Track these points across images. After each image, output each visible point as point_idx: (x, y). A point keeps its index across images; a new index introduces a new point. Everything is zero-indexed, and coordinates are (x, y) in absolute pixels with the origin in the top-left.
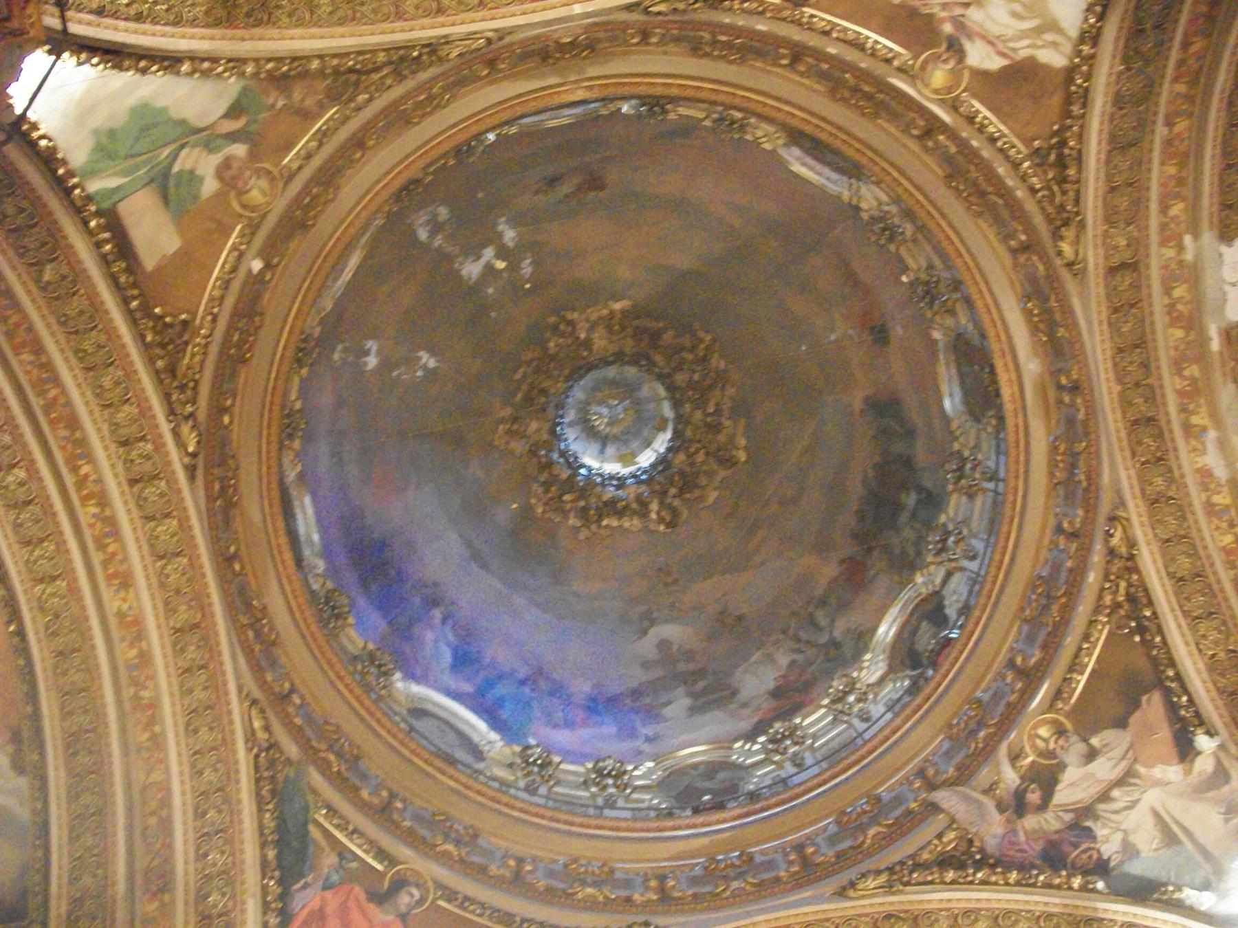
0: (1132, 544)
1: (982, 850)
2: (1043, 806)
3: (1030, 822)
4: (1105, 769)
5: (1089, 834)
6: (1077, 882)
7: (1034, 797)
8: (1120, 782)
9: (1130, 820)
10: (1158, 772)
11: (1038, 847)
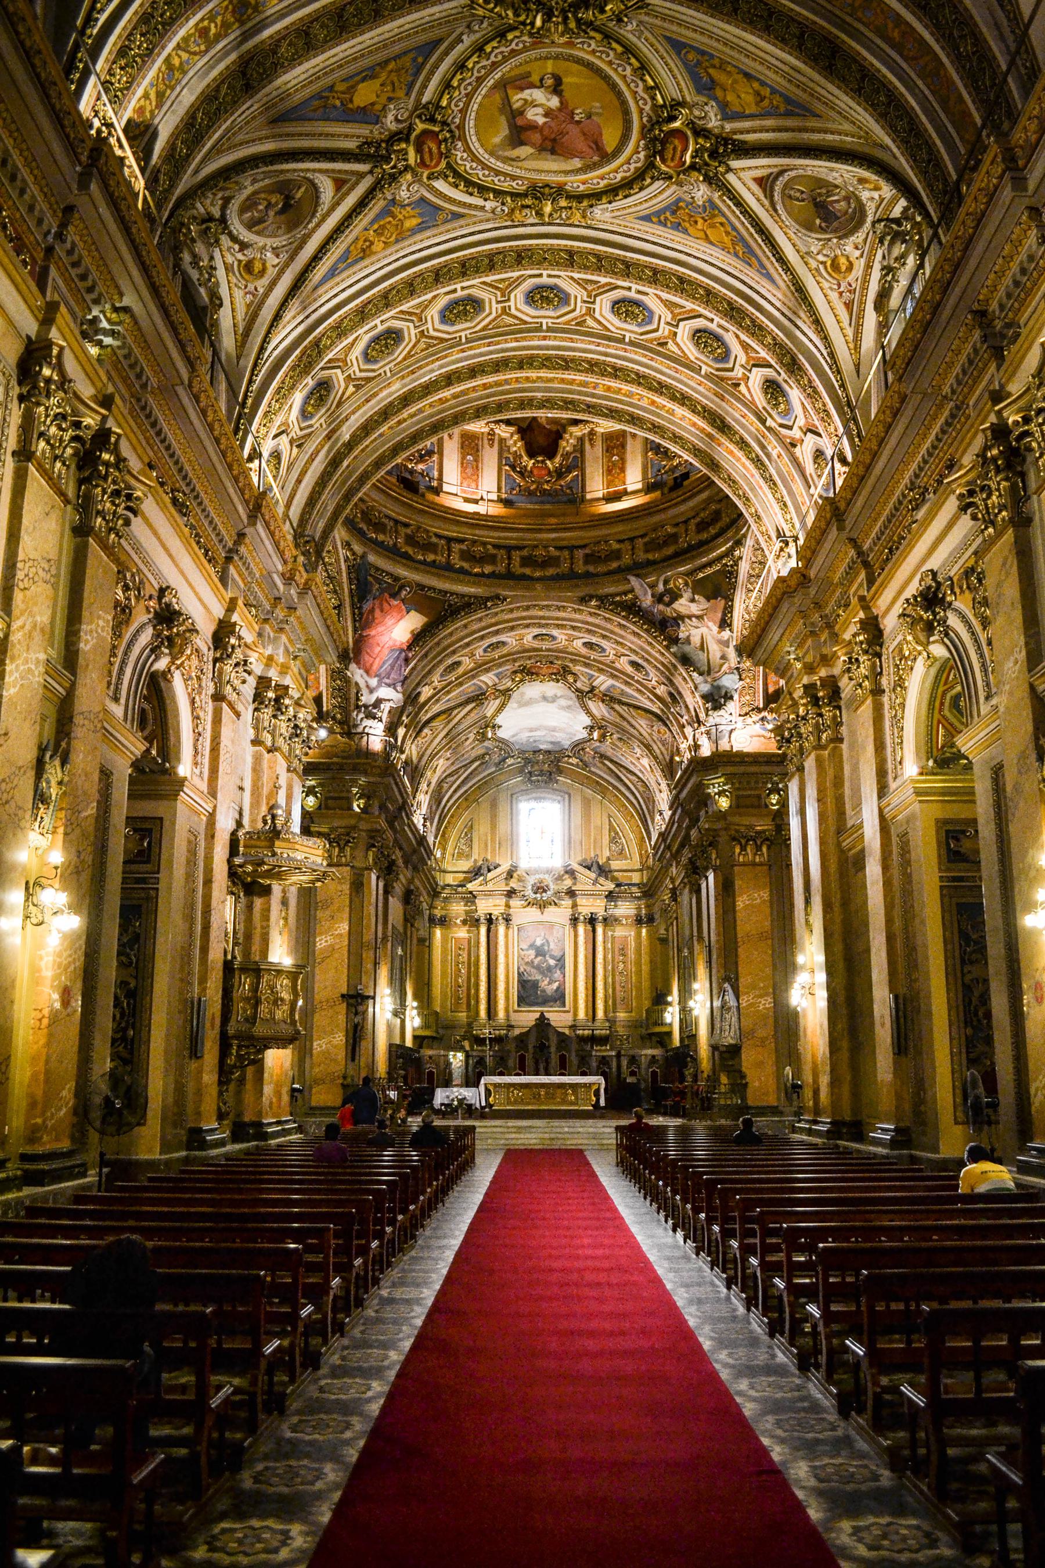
0: (741, 558)
2: (668, 605)
3: (661, 607)
4: (694, 609)
5: (678, 625)
7: (666, 599)
8: (698, 617)
9: (693, 632)
10: (710, 624)
11: (660, 617)
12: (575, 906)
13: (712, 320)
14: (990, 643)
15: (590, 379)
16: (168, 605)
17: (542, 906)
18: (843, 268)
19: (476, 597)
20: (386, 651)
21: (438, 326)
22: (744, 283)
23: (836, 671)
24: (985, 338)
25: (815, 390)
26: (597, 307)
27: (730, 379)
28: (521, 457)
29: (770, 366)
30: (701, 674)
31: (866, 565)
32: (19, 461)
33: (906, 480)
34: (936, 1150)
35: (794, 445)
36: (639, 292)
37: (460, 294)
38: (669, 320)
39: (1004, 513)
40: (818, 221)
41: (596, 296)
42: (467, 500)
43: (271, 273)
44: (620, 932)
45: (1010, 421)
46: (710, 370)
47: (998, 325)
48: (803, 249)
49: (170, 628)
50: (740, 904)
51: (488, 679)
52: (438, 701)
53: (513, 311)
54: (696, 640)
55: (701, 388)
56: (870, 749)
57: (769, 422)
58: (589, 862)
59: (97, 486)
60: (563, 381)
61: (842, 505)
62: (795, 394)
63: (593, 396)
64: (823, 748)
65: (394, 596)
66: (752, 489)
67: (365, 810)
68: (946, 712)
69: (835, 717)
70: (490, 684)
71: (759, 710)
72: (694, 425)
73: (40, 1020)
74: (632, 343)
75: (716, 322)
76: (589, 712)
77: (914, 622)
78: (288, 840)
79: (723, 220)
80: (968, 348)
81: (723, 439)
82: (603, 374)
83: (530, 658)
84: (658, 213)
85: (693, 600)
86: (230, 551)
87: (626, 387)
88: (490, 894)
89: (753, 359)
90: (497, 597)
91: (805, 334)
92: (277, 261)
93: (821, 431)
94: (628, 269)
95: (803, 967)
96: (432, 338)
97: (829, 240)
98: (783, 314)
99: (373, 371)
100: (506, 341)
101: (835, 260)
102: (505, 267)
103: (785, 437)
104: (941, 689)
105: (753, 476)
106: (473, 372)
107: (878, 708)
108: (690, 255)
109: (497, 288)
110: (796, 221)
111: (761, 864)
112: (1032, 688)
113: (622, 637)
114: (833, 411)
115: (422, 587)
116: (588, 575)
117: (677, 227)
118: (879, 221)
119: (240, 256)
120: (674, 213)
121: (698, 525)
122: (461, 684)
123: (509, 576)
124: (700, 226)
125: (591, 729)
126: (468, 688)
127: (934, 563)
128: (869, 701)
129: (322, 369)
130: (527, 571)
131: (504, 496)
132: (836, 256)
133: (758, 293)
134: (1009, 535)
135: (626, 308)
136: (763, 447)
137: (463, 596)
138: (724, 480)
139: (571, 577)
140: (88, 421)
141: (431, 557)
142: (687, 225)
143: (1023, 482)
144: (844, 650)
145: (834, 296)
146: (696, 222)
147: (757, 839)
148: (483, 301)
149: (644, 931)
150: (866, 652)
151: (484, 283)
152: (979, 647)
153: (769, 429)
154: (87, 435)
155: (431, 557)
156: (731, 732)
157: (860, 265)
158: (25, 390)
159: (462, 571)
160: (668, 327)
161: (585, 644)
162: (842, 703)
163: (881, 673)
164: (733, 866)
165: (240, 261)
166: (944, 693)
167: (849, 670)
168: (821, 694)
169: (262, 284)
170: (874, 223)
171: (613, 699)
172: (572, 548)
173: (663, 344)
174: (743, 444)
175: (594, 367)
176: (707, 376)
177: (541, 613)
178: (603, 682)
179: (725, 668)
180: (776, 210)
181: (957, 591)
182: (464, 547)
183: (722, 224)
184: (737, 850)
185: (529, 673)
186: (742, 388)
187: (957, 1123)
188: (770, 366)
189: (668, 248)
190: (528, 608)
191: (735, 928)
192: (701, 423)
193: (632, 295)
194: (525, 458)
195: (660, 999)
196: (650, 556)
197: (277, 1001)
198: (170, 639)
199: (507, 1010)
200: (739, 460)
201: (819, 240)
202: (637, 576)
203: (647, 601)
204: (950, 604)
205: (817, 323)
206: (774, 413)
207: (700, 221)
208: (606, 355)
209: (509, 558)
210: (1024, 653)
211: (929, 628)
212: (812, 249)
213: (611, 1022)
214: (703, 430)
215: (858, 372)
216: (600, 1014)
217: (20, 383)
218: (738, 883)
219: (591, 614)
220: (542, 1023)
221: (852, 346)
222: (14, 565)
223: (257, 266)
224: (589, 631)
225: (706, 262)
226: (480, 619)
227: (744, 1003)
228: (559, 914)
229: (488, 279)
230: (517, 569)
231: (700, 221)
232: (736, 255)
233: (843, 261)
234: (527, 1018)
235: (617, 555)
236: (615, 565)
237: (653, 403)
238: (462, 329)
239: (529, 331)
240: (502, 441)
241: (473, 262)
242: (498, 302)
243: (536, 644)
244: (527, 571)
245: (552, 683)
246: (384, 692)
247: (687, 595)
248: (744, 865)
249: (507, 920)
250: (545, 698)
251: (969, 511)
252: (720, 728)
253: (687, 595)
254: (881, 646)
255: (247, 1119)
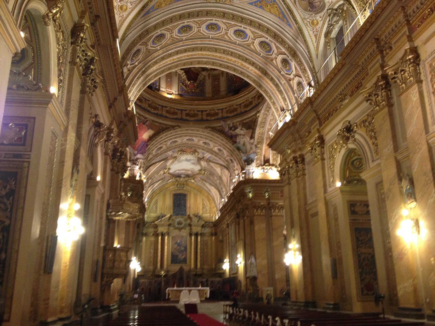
0: (259, 117)
1: (224, 131)
3: (231, 131)
4: (242, 132)
5: (236, 138)
6: (232, 143)
7: (233, 129)
8: (244, 135)
9: (241, 140)
10: (247, 137)
12: (191, 229)
13: (267, 39)
14: (373, 144)
15: (223, 56)
16: (98, 121)
17: (180, 229)
18: (315, 24)
19: (171, 126)
20: (140, 143)
21: (177, 34)
22: (280, 27)
23: (304, 152)
24: (378, 47)
25: (302, 63)
26: (229, 32)
27: (270, 58)
28: (185, 81)
29: (285, 54)
30: (244, 153)
31: (319, 119)
32: (71, 65)
33: (339, 92)
34: (351, 310)
35: (290, 80)
36: (244, 28)
37: (186, 24)
38: (252, 38)
39: (384, 103)
40: (309, 8)
41: (230, 28)
42: (168, 94)
43: (129, 10)
44: (206, 238)
45: (390, 73)
46: (264, 55)
47: (382, 43)
48: (303, 17)
49: (100, 129)
50: (256, 228)
51: (170, 153)
52: (153, 159)
53: (202, 31)
54: (242, 143)
55: (260, 61)
56: (320, 178)
57: (282, 73)
58: (196, 214)
59: (88, 77)
60: (213, 56)
61: (313, 100)
62: (293, 64)
63: (222, 61)
64: (299, 177)
65: (144, 124)
66: (273, 94)
67: (131, 195)
68: (350, 165)
69: (303, 168)
70: (170, 154)
71: (262, 166)
72: (255, 72)
73: (66, 266)
74: (238, 45)
75: (268, 39)
76: (201, 165)
77: (343, 137)
78: (127, 204)
79: (277, 6)
80: (371, 50)
81: (265, 78)
82: (228, 54)
83: (184, 146)
84: (255, 2)
85: (242, 130)
86: (111, 104)
87: (234, 59)
88: (163, 225)
89: (280, 52)
90: (178, 126)
91: (299, 44)
92: (131, 6)
93: (302, 76)
94: (242, 20)
95: (290, 249)
96: (174, 38)
97: (312, 14)
98: (293, 38)
99: (155, 47)
100: (197, 41)
101: (313, 21)
102: (202, 16)
103: (287, 78)
104: (348, 159)
105: (274, 90)
106: (186, 51)
107: (323, 165)
108: (263, 17)
109: (198, 23)
110: (303, 9)
111: (263, 215)
112: (396, 158)
113: (217, 141)
114: (308, 70)
115: (153, 121)
116: (207, 120)
117: (261, 7)
118: (330, 9)
119: (119, 4)
120: (260, 3)
121: (245, 105)
122: (161, 154)
123: (182, 119)
124: (268, 7)
125: (201, 170)
126: (163, 156)
127: (349, 118)
128: (320, 162)
129: (140, 45)
130: (188, 118)
131: (180, 93)
132: (313, 20)
133: (285, 30)
134: (386, 110)
135: (239, 33)
136: (279, 81)
137: (166, 125)
138: (263, 91)
139: (202, 121)
140: (89, 54)
141: (156, 112)
142: (264, 7)
143: (390, 93)
144: (310, 146)
145: (311, 33)
146: (268, 6)
147: (262, 208)
148: (192, 27)
149: (214, 238)
150: (319, 146)
151: (194, 21)
152: (369, 145)
153: (282, 75)
154: (88, 58)
155: (156, 112)
156: (253, 172)
157: (321, 23)
158: (73, 40)
159: (166, 117)
160: (252, 40)
161: (204, 143)
162: (306, 163)
163: (324, 153)
164: (254, 216)
165: (119, 5)
166: (349, 160)
167: (311, 152)
168: (299, 160)
169: (125, 14)
170: (328, 10)
171: (210, 161)
172: (202, 111)
173: (249, 45)
174: (272, 79)
175: (224, 52)
176: (262, 57)
177: (191, 132)
178: (207, 155)
179: (251, 151)
180: (296, 4)
181: (359, 127)
182: (167, 109)
183: (276, 7)
184: (255, 211)
185: (183, 151)
186: (274, 61)
187: (358, 301)
188: (285, 54)
189: (257, 14)
190: (187, 130)
191: (254, 236)
192: (258, 72)
193: (242, 29)
194: (187, 81)
195: (221, 261)
196: (229, 115)
197: (121, 261)
198: (99, 132)
199: (167, 265)
200: (269, 84)
201: (308, 14)
202: (224, 121)
203: (227, 129)
204: (356, 132)
205: (305, 42)
206: (284, 70)
207: (269, 6)
208: (230, 48)
209: (182, 113)
210: (392, 146)
211: (348, 139)
212: (306, 17)
213: (202, 268)
214: (258, 74)
215: (317, 57)
216: (199, 266)
217: (71, 38)
218: (256, 222)
219: (208, 133)
220: (181, 269)
221: (316, 49)
222: (70, 102)
223: (124, 7)
224: (206, 139)
225: (268, 19)
226: (171, 133)
227: (258, 262)
228: (185, 233)
229: (195, 20)
230: (184, 117)
231: (269, 6)
232: (279, 18)
233: (315, 21)
234: (176, 268)
235: (217, 114)
236: (216, 117)
237: (242, 65)
238: (184, 36)
239: (205, 38)
240: (179, 75)
241: (192, 14)
242: (197, 28)
243: (187, 142)
244: (188, 118)
245: (190, 155)
246: (139, 156)
247: (240, 128)
248: (257, 215)
249: (168, 234)
250: (187, 160)
251: (369, 102)
252: (250, 171)
253: (240, 128)
254: (324, 144)
255: (105, 304)
